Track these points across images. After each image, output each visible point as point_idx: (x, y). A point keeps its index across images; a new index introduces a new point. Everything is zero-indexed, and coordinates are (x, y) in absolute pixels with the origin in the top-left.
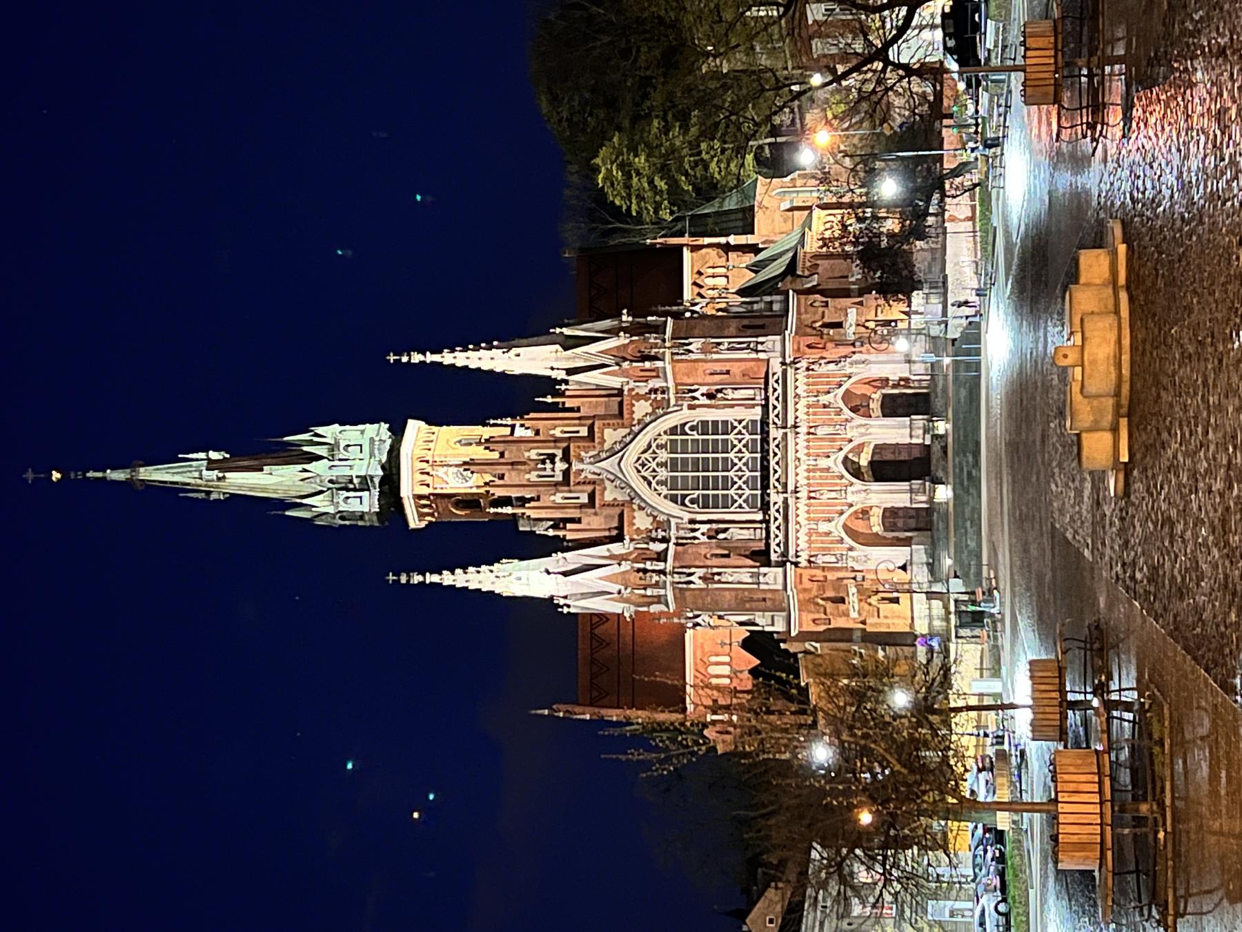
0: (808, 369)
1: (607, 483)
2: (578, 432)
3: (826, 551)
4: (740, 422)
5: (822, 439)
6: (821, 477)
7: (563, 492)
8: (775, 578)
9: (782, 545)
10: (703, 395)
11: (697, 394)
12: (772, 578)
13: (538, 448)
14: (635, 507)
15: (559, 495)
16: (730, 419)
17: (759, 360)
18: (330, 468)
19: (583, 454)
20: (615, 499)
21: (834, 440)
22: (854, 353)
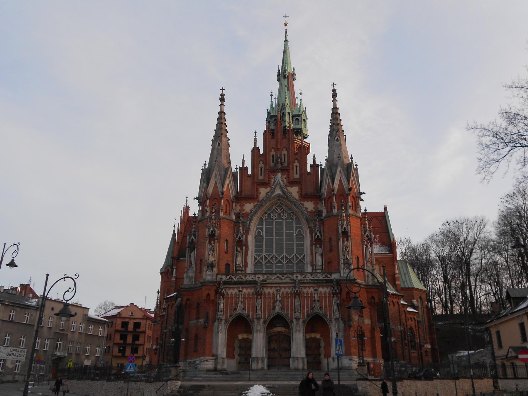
0: (334, 294)
1: (269, 189)
2: (297, 173)
3: (226, 305)
4: (303, 258)
5: (292, 303)
6: (269, 302)
7: (265, 166)
8: (209, 275)
9: (230, 280)
10: (318, 237)
11: (318, 234)
12: (210, 273)
13: (288, 154)
14: (256, 203)
15: (263, 165)
16: (305, 253)
17: (339, 265)
18: (289, 113)
19: (285, 176)
20: (260, 193)
21: (292, 310)
22: (344, 322)
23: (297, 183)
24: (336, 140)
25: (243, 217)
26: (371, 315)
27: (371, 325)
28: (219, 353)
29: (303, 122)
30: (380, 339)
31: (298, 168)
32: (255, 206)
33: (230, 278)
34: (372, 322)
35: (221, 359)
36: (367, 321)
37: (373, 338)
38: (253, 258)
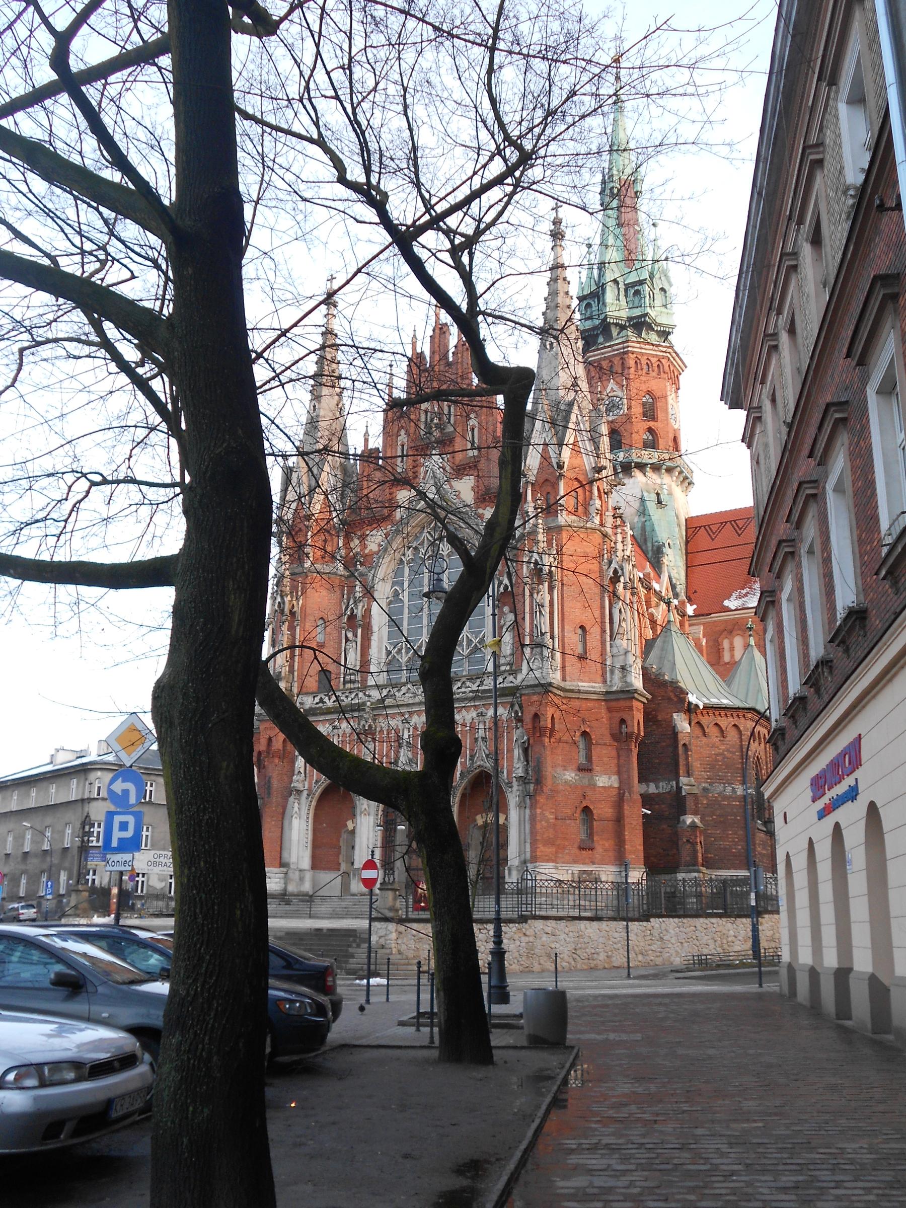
9: (321, 705)
16: (485, 630)
23: (470, 467)
24: (548, 347)
25: (361, 564)
26: (619, 766)
27: (619, 788)
28: (293, 859)
29: (658, 296)
30: (641, 820)
31: (476, 430)
32: (387, 535)
33: (321, 701)
34: (620, 782)
35: (297, 873)
36: (605, 780)
37: (619, 820)
38: (384, 651)
